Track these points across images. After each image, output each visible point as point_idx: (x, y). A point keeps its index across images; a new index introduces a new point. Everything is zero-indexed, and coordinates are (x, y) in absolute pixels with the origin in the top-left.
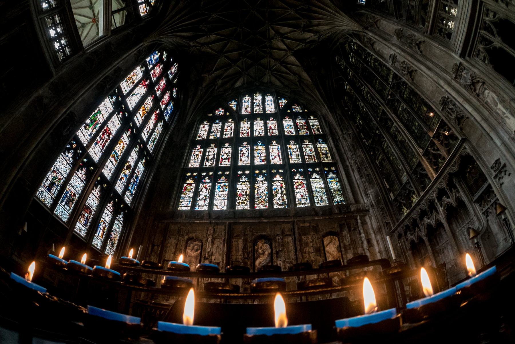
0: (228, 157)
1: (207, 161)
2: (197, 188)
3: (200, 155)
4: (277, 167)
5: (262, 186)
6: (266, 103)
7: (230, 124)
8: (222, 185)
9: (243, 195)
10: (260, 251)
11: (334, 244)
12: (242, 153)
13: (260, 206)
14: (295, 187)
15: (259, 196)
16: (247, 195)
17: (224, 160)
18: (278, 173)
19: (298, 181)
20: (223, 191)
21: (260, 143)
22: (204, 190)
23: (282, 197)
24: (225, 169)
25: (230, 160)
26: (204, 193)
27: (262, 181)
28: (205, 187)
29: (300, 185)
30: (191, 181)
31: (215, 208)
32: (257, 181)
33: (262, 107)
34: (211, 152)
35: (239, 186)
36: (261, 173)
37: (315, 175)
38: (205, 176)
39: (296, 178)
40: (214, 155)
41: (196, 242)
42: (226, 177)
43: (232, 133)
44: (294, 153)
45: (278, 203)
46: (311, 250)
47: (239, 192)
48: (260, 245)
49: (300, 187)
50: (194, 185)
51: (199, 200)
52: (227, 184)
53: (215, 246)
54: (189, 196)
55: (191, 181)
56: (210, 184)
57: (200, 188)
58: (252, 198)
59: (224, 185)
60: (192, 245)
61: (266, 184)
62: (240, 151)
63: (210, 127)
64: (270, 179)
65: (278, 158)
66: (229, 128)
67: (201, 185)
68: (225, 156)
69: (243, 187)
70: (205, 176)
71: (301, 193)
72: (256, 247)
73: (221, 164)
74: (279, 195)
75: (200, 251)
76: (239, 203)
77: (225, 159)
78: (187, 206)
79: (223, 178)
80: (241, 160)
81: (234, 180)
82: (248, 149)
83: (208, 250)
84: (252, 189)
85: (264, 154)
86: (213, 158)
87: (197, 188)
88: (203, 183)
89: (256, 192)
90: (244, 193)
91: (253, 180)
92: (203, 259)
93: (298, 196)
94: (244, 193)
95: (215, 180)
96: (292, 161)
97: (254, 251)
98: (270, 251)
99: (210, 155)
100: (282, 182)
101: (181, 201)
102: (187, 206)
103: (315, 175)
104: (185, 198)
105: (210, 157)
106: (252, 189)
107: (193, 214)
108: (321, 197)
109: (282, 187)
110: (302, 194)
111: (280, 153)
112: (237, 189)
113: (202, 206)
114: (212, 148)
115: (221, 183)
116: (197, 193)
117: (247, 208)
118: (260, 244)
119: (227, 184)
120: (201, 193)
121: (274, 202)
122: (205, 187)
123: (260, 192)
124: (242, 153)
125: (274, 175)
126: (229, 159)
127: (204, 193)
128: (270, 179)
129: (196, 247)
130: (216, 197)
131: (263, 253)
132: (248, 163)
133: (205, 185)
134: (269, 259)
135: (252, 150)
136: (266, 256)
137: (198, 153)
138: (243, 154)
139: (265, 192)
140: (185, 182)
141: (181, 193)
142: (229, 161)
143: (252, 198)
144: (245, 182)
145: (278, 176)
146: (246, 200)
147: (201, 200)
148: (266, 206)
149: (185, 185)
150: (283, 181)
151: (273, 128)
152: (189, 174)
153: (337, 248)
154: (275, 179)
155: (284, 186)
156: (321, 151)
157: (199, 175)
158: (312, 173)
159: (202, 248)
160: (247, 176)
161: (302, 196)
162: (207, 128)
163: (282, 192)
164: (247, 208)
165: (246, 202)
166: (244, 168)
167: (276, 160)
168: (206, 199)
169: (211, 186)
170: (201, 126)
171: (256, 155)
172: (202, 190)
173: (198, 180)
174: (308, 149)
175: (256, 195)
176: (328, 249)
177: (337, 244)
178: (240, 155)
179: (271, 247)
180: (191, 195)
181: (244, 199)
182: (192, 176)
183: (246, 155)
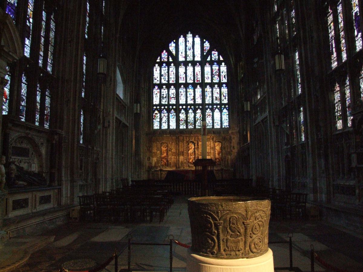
0: (174, 96)
1: (163, 99)
2: (161, 116)
3: (158, 94)
4: (199, 105)
5: (191, 115)
6: (195, 47)
7: (173, 68)
8: (173, 114)
9: (183, 120)
10: (190, 147)
11: (219, 146)
12: (181, 94)
13: (190, 127)
14: (206, 117)
15: (190, 121)
16: (184, 120)
17: (172, 99)
18: (199, 108)
19: (208, 113)
20: (173, 118)
21: (190, 86)
22: (164, 117)
23: (200, 122)
24: (173, 105)
25: (175, 99)
26: (164, 119)
27: (191, 113)
28: (165, 116)
29: (209, 115)
30: (156, 112)
31: (171, 128)
32: (189, 113)
33: (192, 51)
34: (164, 92)
35: (181, 115)
36: (191, 108)
37: (217, 110)
38: (163, 109)
39: (207, 111)
40: (166, 94)
41: (165, 144)
42: (174, 109)
43: (175, 78)
44: (208, 95)
45: (198, 125)
46: (209, 148)
47: (181, 118)
48: (190, 145)
49: (209, 116)
50: (159, 114)
51: (163, 123)
52: (175, 114)
53: (173, 146)
54: (157, 120)
55: (156, 112)
56: (167, 114)
57: (162, 116)
58: (187, 122)
59: (174, 115)
60: (163, 145)
61: (193, 114)
62: (180, 92)
63: (161, 70)
64: (195, 112)
65: (199, 98)
66: (172, 73)
67: (162, 114)
68: (172, 96)
69: (182, 116)
70: (163, 109)
71: (209, 120)
72: (189, 146)
73: (171, 101)
74: (199, 121)
75: (167, 148)
76: (181, 125)
77: (172, 98)
78: (157, 126)
79: (173, 110)
80: (181, 99)
81: (178, 111)
82: (184, 91)
83: (170, 147)
84: (187, 117)
85: (193, 95)
86: (166, 97)
87: (161, 116)
88: (163, 113)
89: (188, 119)
90: (183, 119)
91: (187, 113)
92: (168, 151)
93: (207, 121)
94: (183, 119)
95: (169, 111)
96: (207, 102)
97: (188, 147)
98: (194, 147)
99: (163, 95)
100: (200, 114)
101: (154, 123)
102: (157, 126)
103: (217, 110)
104: (156, 122)
105: (165, 96)
106: (187, 117)
107: (161, 132)
108: (218, 123)
109: (200, 117)
110: (209, 121)
111: (201, 95)
112: (180, 117)
113: (165, 126)
114: (164, 89)
115: (172, 113)
116: (161, 119)
117: (185, 128)
118: (190, 144)
119: (175, 114)
120: (163, 119)
121: (196, 124)
122: (165, 116)
123: (190, 119)
124: (181, 94)
125: (197, 110)
126: (174, 97)
127: (164, 119)
128: (195, 112)
129: (165, 146)
130: (170, 121)
131: (191, 148)
132: (184, 103)
133: (164, 114)
134: (193, 151)
135: (186, 92)
136: (192, 149)
137: (156, 92)
138: (182, 94)
139: (193, 119)
140: (154, 113)
141: (153, 119)
142: (174, 99)
143: (187, 122)
144: (183, 113)
145: (199, 110)
146: (184, 123)
147: (164, 123)
148: (193, 126)
149: (154, 114)
150: (201, 113)
151: (198, 74)
152: (155, 107)
153: (220, 148)
154: (197, 112)
155: (201, 116)
156: (223, 93)
157: (160, 108)
158: (216, 108)
159: (167, 146)
160: (184, 109)
161: (209, 122)
162: (158, 71)
163: (200, 119)
164: (185, 128)
165: (184, 124)
166: (182, 105)
167: (199, 101)
168: (166, 123)
169: (168, 115)
170: (155, 69)
171: (188, 95)
172: (163, 118)
173: (160, 111)
174: (216, 92)
175: (188, 120)
176: (216, 148)
177: (220, 146)
178: (180, 95)
179: (195, 146)
180: (159, 120)
181: (183, 122)
182: (156, 109)
183: (183, 95)
